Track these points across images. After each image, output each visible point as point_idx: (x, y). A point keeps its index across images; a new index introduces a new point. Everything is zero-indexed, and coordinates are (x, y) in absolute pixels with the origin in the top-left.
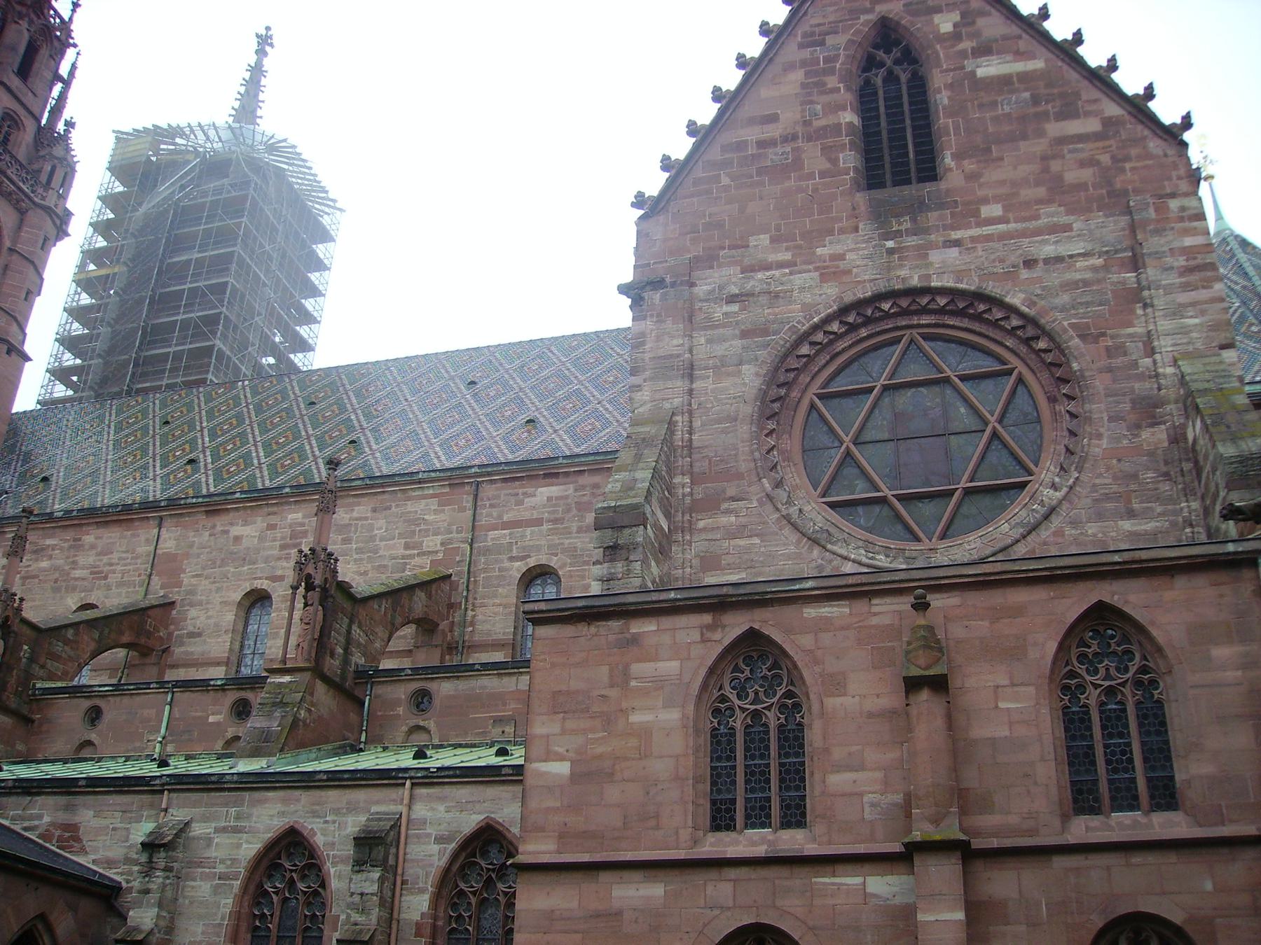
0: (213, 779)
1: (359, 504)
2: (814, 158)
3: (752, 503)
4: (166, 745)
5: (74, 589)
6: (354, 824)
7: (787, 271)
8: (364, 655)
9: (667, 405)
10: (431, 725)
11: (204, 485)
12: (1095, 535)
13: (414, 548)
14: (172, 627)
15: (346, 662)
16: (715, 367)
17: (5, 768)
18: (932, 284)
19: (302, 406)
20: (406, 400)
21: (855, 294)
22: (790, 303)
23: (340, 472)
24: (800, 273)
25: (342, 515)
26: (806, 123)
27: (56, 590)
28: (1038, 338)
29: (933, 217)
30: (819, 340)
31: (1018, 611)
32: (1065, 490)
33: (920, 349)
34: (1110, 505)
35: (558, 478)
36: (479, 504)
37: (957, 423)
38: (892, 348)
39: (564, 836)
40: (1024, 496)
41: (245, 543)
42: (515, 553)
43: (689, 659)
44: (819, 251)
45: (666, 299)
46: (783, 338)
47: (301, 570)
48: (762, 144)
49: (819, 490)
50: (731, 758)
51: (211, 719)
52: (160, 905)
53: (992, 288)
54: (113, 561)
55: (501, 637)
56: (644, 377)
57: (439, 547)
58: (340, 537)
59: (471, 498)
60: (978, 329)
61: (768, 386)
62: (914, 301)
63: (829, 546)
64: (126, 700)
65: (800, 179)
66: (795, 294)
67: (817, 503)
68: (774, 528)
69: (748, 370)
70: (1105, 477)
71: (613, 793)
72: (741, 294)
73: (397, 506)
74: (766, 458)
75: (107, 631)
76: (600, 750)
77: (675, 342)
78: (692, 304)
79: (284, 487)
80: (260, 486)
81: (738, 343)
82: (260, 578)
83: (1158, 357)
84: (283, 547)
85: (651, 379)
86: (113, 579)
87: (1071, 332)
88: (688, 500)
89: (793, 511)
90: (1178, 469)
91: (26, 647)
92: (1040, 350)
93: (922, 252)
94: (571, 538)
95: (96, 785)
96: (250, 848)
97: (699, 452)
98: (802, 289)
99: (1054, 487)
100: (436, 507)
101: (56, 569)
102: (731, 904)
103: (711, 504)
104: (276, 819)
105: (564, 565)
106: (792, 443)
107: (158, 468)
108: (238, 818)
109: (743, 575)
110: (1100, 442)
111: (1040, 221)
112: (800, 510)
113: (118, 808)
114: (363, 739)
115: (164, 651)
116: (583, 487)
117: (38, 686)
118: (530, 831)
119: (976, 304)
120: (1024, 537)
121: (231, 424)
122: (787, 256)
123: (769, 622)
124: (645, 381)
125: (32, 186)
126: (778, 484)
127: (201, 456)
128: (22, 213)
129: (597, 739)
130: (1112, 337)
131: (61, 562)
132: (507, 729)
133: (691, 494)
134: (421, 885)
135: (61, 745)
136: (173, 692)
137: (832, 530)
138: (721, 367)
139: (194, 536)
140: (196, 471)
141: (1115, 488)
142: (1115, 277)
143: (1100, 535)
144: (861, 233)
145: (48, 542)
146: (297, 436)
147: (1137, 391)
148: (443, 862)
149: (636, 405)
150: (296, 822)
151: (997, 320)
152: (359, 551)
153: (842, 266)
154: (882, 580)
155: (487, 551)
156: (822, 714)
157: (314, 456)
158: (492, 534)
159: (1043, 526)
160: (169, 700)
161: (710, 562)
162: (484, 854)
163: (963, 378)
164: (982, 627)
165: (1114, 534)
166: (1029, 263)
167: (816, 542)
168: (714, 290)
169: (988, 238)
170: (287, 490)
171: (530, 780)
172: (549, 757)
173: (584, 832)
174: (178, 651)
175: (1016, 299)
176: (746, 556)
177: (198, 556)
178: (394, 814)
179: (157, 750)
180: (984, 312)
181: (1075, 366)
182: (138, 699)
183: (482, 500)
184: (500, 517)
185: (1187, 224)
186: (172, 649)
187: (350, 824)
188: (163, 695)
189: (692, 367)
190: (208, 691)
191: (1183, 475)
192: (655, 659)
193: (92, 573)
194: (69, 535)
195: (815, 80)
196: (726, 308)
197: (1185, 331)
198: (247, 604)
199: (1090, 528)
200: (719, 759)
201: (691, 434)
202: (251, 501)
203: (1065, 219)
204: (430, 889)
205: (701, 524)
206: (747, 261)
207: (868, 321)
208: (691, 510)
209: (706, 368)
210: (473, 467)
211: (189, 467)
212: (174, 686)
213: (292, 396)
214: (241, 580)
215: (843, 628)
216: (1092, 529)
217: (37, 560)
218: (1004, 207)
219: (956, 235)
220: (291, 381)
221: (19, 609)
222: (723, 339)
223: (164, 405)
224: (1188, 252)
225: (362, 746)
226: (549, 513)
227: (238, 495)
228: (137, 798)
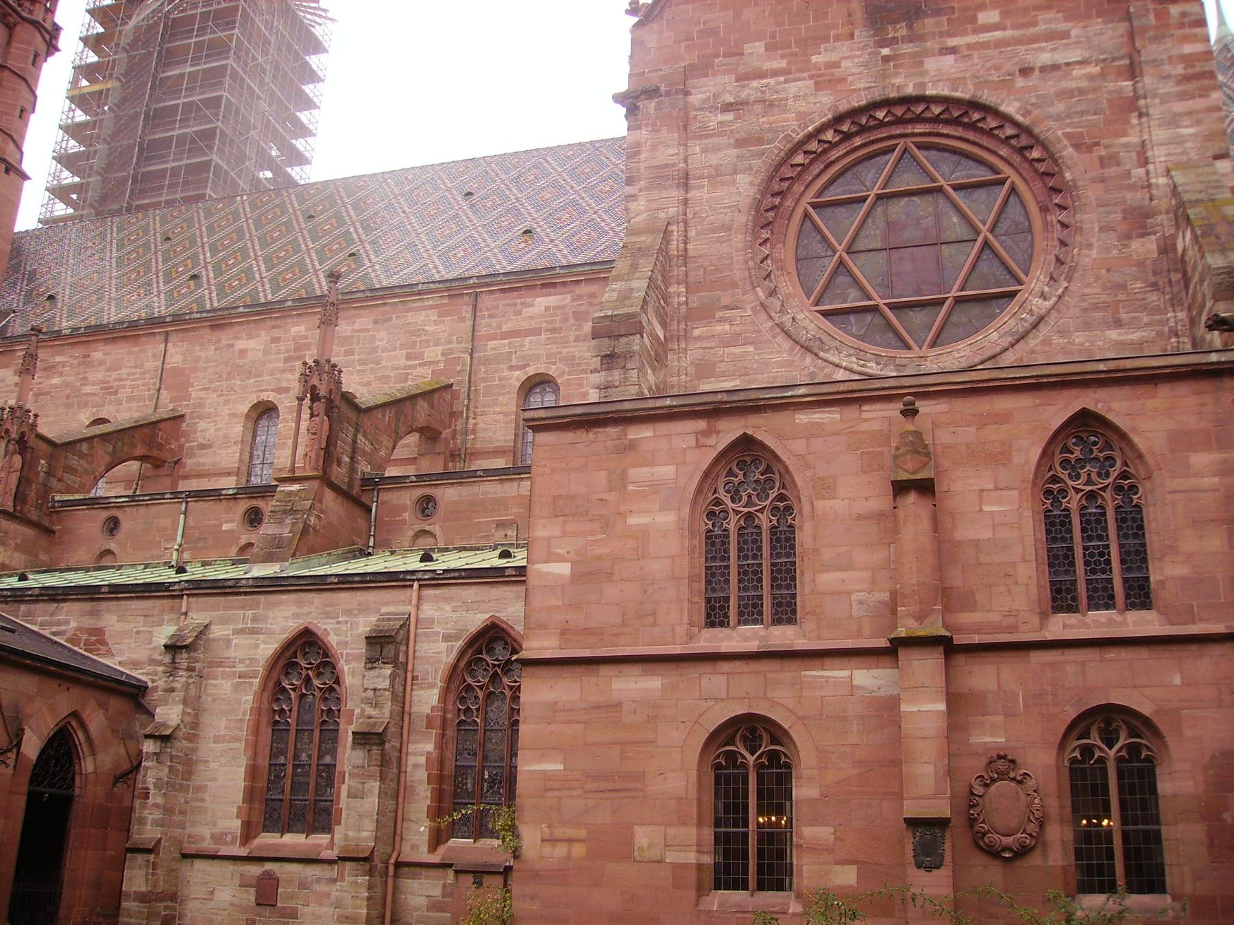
0: (230, 583)
1: (360, 316)
4: (182, 552)
5: (86, 404)
6: (365, 624)
7: (782, 79)
9: (662, 215)
10: (436, 529)
12: (1082, 344)
13: (415, 359)
14: (183, 440)
15: (352, 470)
16: (710, 177)
17: (31, 577)
18: (927, 93)
19: (301, 220)
20: (404, 212)
21: (849, 102)
23: (341, 285)
24: (795, 80)
25: (344, 328)
27: (68, 406)
28: (1032, 147)
29: (929, 24)
31: (1002, 418)
32: (1054, 299)
33: (914, 158)
34: (1098, 315)
36: (478, 314)
37: (949, 233)
38: (887, 157)
39: (564, 633)
40: (1014, 305)
41: (250, 356)
43: (684, 463)
44: (814, 59)
45: (661, 109)
46: (778, 147)
47: (306, 381)
49: (812, 298)
50: (725, 558)
51: (225, 527)
52: (185, 703)
53: (987, 97)
54: (123, 376)
55: (502, 444)
56: (639, 186)
57: (440, 358)
58: (343, 349)
59: (470, 309)
60: (972, 138)
61: (763, 196)
62: (909, 109)
63: (822, 354)
64: (142, 510)
66: (790, 102)
67: (810, 311)
68: (768, 336)
69: (743, 179)
70: (1094, 287)
71: (612, 592)
73: (398, 317)
74: (760, 267)
75: (119, 444)
76: (598, 551)
77: (670, 151)
78: (687, 113)
80: (263, 300)
81: (733, 152)
82: (267, 390)
83: (1151, 167)
84: (287, 360)
85: (647, 189)
86: (123, 394)
87: (1065, 142)
88: (683, 308)
89: (787, 319)
90: (1166, 280)
91: (43, 462)
92: (1034, 160)
93: (918, 60)
95: (119, 592)
96: (267, 648)
97: (695, 262)
98: (797, 98)
99: (1043, 296)
100: (436, 318)
101: (68, 385)
102: (725, 696)
103: (705, 313)
105: (562, 374)
106: (786, 252)
107: (161, 284)
108: (254, 619)
110: (1091, 252)
111: (1037, 29)
112: (793, 318)
114: (371, 544)
115: (176, 463)
116: (580, 297)
117: (57, 498)
118: (533, 629)
119: (971, 113)
120: (1013, 345)
121: (231, 239)
122: (783, 64)
123: (762, 428)
124: (640, 190)
126: (772, 293)
127: (204, 272)
129: (596, 541)
130: (1106, 147)
132: (509, 533)
133: (687, 303)
134: (430, 680)
135: (82, 555)
136: (187, 502)
137: (825, 338)
138: (716, 176)
139: (201, 351)
140: (199, 286)
141: (1103, 298)
142: (1111, 86)
143: (1087, 344)
144: (856, 40)
145: (58, 359)
146: (297, 249)
147: (1129, 202)
148: (451, 659)
149: (632, 215)
151: (991, 129)
152: (362, 362)
153: (837, 75)
154: (872, 387)
155: (487, 361)
156: (813, 516)
157: (314, 268)
158: (491, 344)
159: (1031, 335)
160: (183, 509)
161: (705, 369)
162: (490, 651)
163: (956, 188)
164: (968, 434)
165: (1100, 343)
166: (1025, 71)
167: (808, 349)
168: (709, 99)
169: (985, 45)
170: (290, 303)
171: (532, 579)
172: (551, 558)
174: (189, 463)
175: (1010, 108)
176: (741, 364)
177: (205, 369)
178: (403, 614)
179: (175, 556)
180: (979, 121)
181: (1068, 176)
182: (153, 509)
183: (481, 310)
184: (499, 326)
185: (1187, 31)
186: (184, 460)
187: (361, 624)
188: (177, 505)
189: (687, 177)
191: (1171, 286)
192: (652, 463)
193: (102, 389)
194: (78, 351)
196: (721, 117)
197: (1179, 141)
198: (255, 415)
199: (1078, 337)
200: (714, 559)
201: (686, 244)
202: (255, 315)
203: (1063, 26)
204: (439, 684)
205: (696, 333)
206: (741, 70)
207: (863, 130)
208: (686, 319)
209: (701, 177)
210: (471, 277)
212: (188, 496)
213: (291, 211)
214: (246, 393)
215: (833, 434)
216: (1079, 338)
217: (48, 377)
218: (1001, 13)
219: (952, 42)
220: (289, 194)
221: (34, 425)
223: (164, 222)
224: (1188, 60)
225: (370, 550)
226: (547, 322)
227: (241, 309)
228: (158, 602)
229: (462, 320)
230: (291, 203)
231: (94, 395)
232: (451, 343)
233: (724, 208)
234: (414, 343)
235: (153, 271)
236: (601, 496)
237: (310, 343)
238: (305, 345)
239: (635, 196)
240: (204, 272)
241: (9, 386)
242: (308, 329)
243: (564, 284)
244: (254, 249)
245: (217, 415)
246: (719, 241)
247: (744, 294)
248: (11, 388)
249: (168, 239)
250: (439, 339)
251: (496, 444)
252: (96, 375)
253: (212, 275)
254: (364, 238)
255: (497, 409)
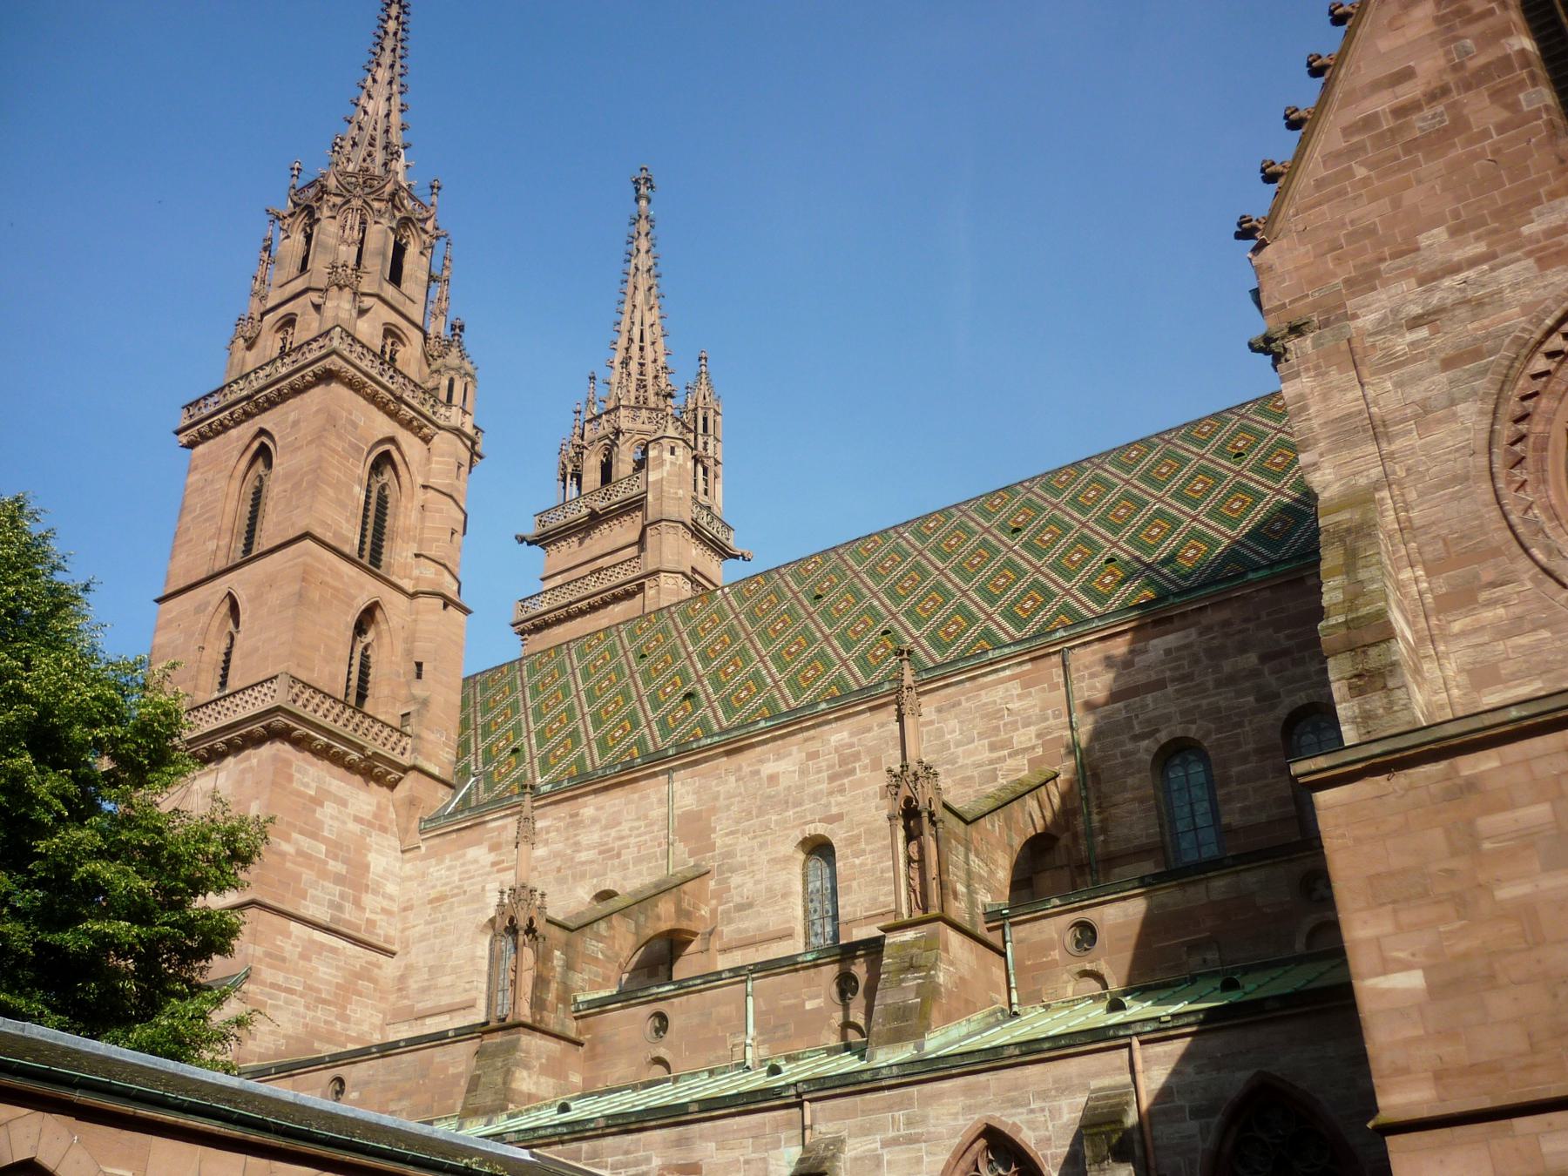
0: (866, 1076)
2: (1482, 110)
3: (1523, 585)
5: (583, 876)
6: (1070, 1111)
7: (1485, 267)
8: (989, 891)
9: (1362, 481)
11: (713, 721)
13: (1002, 748)
15: (972, 903)
16: (1417, 416)
19: (806, 603)
22: (1502, 307)
24: (1505, 265)
26: (1457, 68)
30: (1559, 348)
35: (1172, 622)
41: (784, 782)
42: (1137, 730)
44: (1526, 230)
48: (1400, 112)
51: (809, 1006)
54: (624, 833)
55: (1144, 841)
65: (1471, 141)
66: (1508, 294)
71: (1500, 1004)
72: (1428, 313)
73: (968, 700)
75: (642, 919)
76: (1462, 946)
79: (818, 703)
80: (785, 709)
81: (1442, 377)
82: (812, 822)
84: (832, 778)
85: (1330, 451)
86: (627, 855)
88: (1429, 598)
94: (1208, 696)
95: (713, 1108)
97: (1426, 533)
98: (1515, 286)
100: (1019, 691)
101: (557, 855)
104: (960, 1117)
105: (1208, 733)
108: (910, 1123)
109: (1538, 684)
113: (746, 1134)
114: (1015, 999)
115: (711, 934)
116: (1209, 629)
117: (580, 999)
122: (1481, 248)
124: (1321, 455)
125: (433, 406)
127: (698, 687)
128: (426, 440)
129: (1451, 932)
131: (559, 846)
132: (1209, 956)
138: (1424, 414)
139: (717, 785)
140: (696, 707)
146: (812, 640)
150: (990, 1117)
157: (841, 658)
168: (1385, 318)
170: (823, 706)
172: (1387, 966)
173: (1472, 1066)
176: (1536, 658)
177: (728, 807)
187: (1065, 1110)
190: (796, 970)
192: (1509, 805)
194: (564, 810)
195: (1454, 7)
196: (1411, 337)
202: (780, 728)
206: (1422, 269)
209: (1405, 420)
211: (687, 703)
212: (752, 972)
213: (790, 595)
214: (786, 829)
220: (782, 576)
221: (542, 908)
222: (1417, 378)
227: (762, 724)
229: (1054, 687)
230: (787, 585)
231: (592, 862)
232: (1047, 719)
233: (1450, 453)
234: (997, 728)
235: (635, 698)
236: (1446, 865)
237: (859, 753)
238: (853, 755)
239: (1315, 464)
240: (698, 687)
241: (484, 867)
242: (852, 735)
243: (1183, 615)
244: (755, 648)
245: (752, 863)
246: (1454, 498)
247: (1512, 561)
248: (488, 869)
249: (643, 656)
250: (1029, 717)
251: (1136, 842)
252: (590, 837)
253: (710, 690)
254: (894, 609)
255: (1128, 795)
